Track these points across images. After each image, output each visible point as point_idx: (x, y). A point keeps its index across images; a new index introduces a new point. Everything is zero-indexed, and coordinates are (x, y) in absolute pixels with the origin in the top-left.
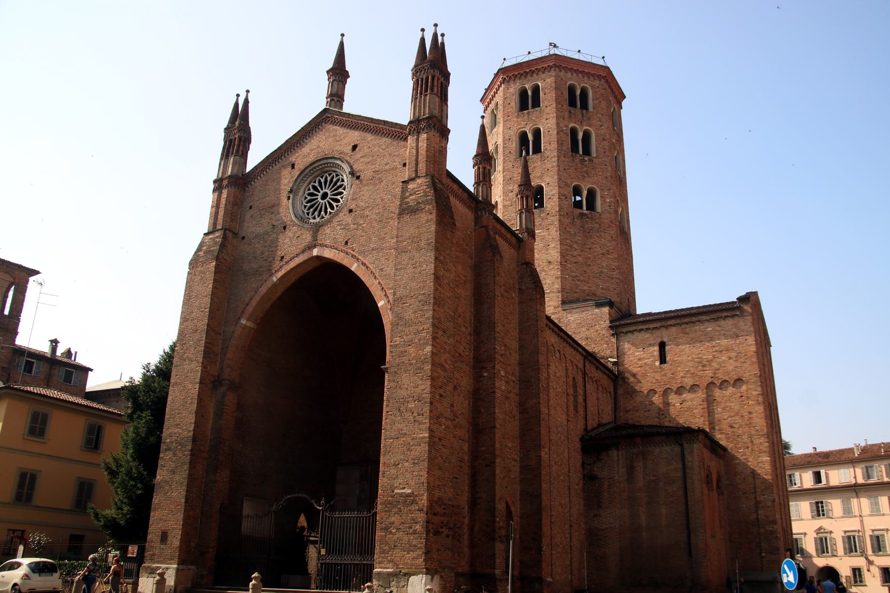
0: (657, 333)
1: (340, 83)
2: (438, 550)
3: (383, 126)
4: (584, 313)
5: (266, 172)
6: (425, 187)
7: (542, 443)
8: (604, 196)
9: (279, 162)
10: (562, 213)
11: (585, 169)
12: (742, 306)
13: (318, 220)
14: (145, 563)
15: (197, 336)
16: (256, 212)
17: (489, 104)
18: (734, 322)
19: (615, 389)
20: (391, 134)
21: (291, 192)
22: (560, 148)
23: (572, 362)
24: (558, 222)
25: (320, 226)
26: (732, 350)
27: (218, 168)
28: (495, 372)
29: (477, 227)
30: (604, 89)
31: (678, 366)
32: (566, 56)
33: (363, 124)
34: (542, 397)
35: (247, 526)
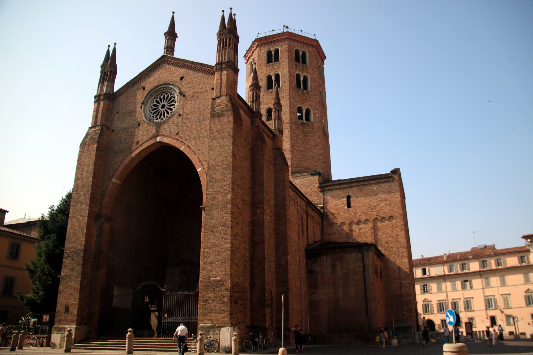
0: (346, 190)
1: (173, 41)
2: (237, 313)
3: (199, 66)
4: (304, 179)
5: (127, 92)
6: (226, 102)
7: (288, 251)
8: (315, 113)
9: (135, 86)
10: (292, 122)
11: (305, 97)
12: (393, 176)
13: (159, 120)
14: (55, 325)
15: (86, 189)
16: (121, 115)
17: (249, 59)
18: (388, 185)
19: (322, 222)
20: (204, 71)
21: (143, 103)
22: (290, 85)
23: (301, 206)
24: (289, 127)
25: (161, 124)
26: (388, 200)
27: (97, 89)
28: (264, 210)
29: (252, 127)
30: (315, 53)
31: (358, 209)
32: (294, 33)
33: (187, 65)
34: (288, 226)
35: (116, 302)
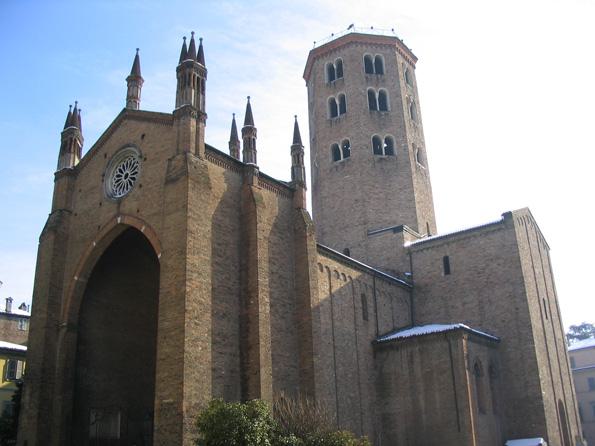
19: (412, 300)
